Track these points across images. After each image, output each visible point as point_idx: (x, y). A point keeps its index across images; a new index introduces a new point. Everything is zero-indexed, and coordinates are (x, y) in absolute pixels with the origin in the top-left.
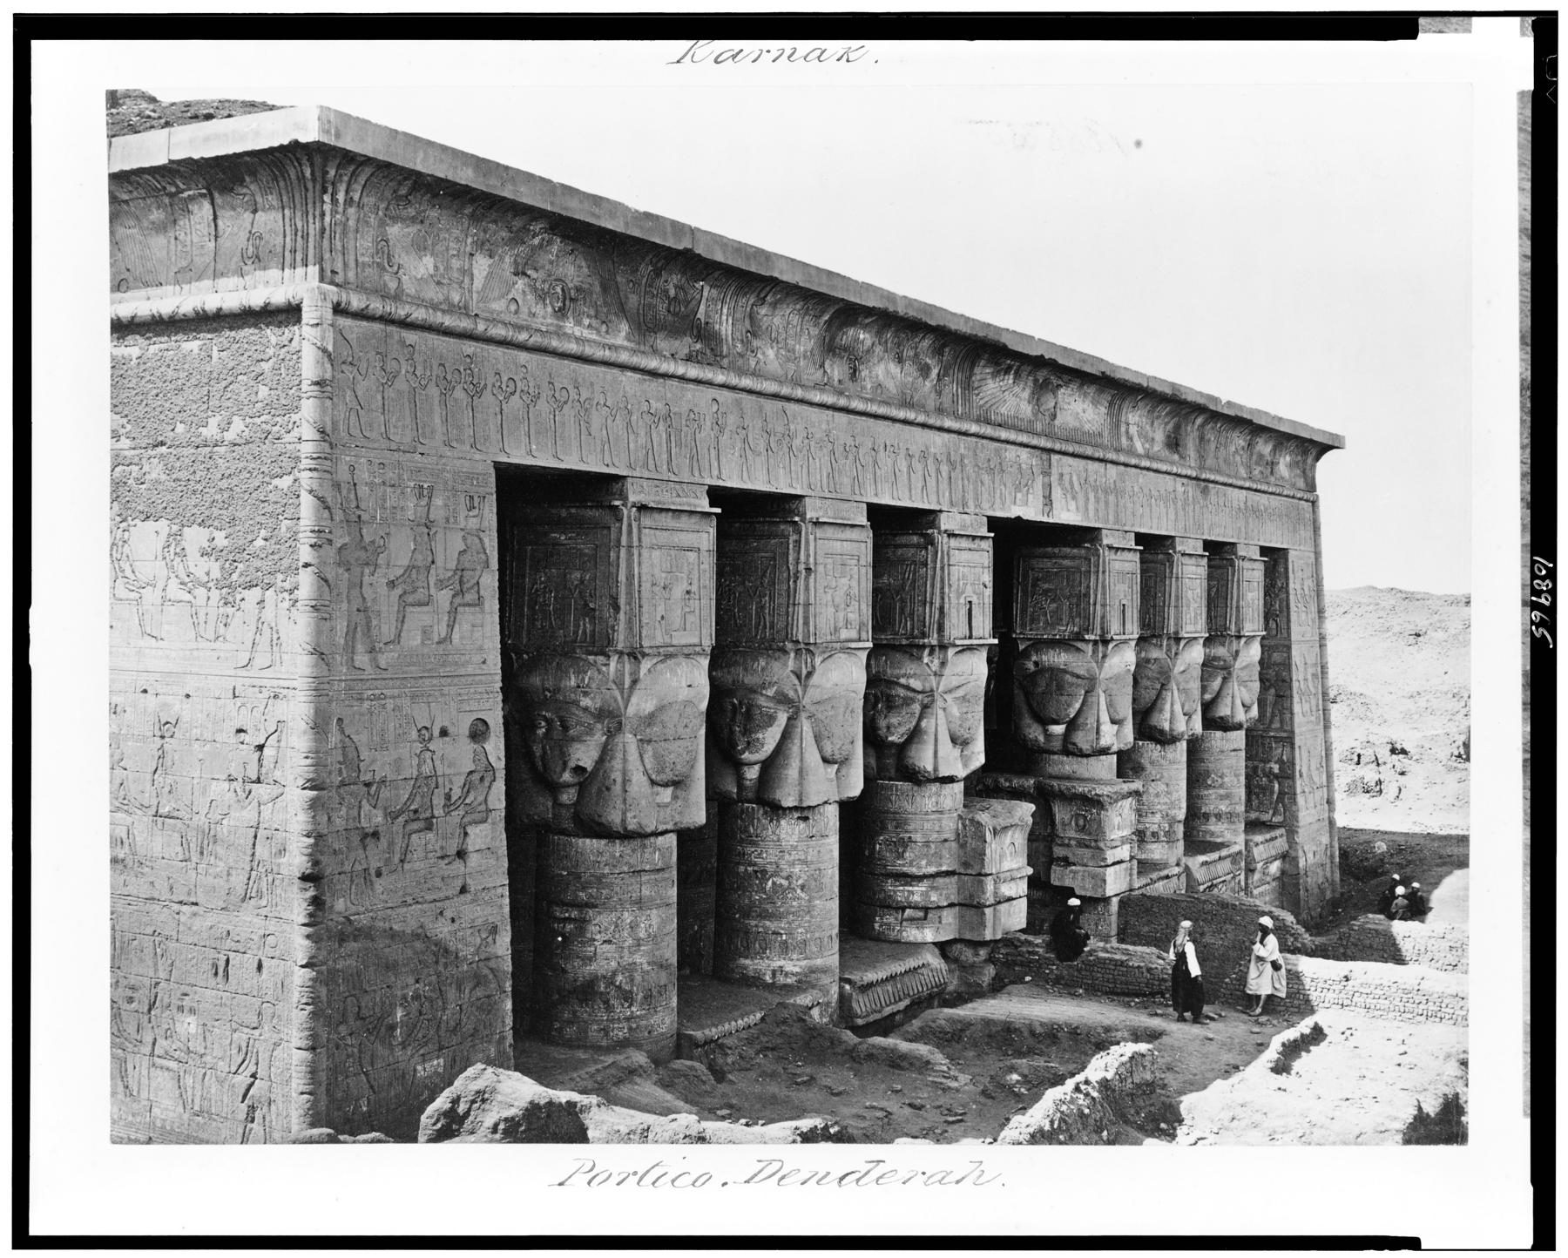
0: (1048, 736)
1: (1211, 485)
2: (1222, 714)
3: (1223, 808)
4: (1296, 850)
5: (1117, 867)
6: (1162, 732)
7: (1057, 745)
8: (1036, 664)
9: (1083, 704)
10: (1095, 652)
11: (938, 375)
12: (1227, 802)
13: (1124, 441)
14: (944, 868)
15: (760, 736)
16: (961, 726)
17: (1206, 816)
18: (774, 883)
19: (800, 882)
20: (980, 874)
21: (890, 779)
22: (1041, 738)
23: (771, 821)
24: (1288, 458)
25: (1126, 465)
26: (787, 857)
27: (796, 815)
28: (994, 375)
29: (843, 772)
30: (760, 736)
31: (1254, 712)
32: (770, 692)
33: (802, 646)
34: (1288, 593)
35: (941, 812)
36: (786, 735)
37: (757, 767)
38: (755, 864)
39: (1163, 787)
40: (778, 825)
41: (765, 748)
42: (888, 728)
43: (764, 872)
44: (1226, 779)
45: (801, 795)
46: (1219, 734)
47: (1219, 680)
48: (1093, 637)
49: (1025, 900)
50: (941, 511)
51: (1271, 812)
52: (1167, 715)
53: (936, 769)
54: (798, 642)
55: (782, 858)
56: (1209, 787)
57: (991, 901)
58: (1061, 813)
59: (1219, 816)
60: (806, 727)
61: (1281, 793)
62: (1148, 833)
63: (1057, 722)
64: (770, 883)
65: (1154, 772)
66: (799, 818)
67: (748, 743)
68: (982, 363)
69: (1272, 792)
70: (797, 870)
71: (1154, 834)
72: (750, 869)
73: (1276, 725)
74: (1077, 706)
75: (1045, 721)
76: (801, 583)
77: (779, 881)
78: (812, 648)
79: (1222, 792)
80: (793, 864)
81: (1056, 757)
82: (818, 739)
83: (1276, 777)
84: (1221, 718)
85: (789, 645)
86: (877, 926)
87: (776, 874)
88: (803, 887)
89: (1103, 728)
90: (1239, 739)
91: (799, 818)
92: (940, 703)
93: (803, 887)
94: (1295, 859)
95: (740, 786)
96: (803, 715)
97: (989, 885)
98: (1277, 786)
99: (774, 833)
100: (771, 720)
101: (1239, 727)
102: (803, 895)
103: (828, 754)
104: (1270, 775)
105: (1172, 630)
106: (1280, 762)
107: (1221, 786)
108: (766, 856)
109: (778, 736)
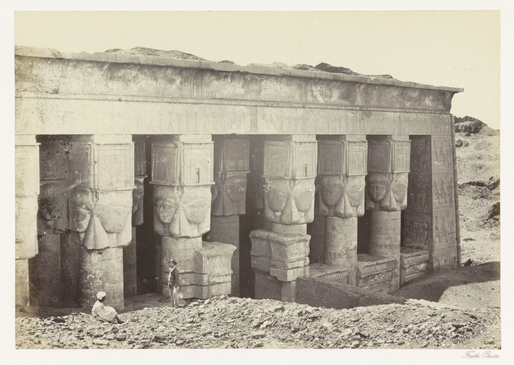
0: (275, 216)
1: (373, 112)
2: (386, 205)
3: (388, 242)
4: (432, 260)
5: (295, 270)
6: (340, 214)
7: (278, 220)
8: (270, 188)
9: (286, 203)
10: (290, 184)
11: (181, 82)
12: (389, 241)
13: (310, 99)
14: (187, 271)
15: (81, 222)
16: (191, 217)
17: (381, 246)
18: (90, 276)
19: (99, 276)
20: (201, 274)
21: (168, 237)
22: (273, 217)
23: (88, 254)
24: (431, 98)
25: (310, 108)
26: (94, 267)
27: (97, 252)
28: (218, 79)
29: (119, 236)
30: (81, 222)
31: (405, 203)
32: (84, 206)
33: (94, 190)
34: (431, 153)
35: (186, 250)
36: (90, 222)
37: (84, 234)
38: (84, 269)
39: (343, 236)
40: (91, 256)
41: (84, 227)
42: (164, 217)
43: (87, 272)
44: (389, 231)
45: (95, 245)
46: (386, 213)
47: (385, 191)
48: (288, 178)
49: (230, 283)
50: (181, 134)
51: (424, 243)
52: (343, 207)
53: (180, 234)
54: (91, 189)
55: (92, 267)
56: (382, 234)
57: (207, 284)
58: (273, 247)
59: (386, 246)
60: (97, 221)
61: (427, 236)
62: (337, 254)
63: (277, 211)
64: (88, 277)
65: (339, 230)
66: (98, 253)
67: (78, 225)
68: (208, 75)
69: (424, 235)
70: (98, 272)
71: (339, 255)
72: (83, 271)
73: (426, 208)
74: (284, 205)
75: (274, 211)
76: (92, 167)
77: (91, 276)
78: (97, 191)
79: (387, 236)
80: (96, 270)
81: (278, 225)
82: (103, 224)
83: (426, 229)
84: (386, 206)
85: (89, 190)
86: (164, 291)
87: (90, 273)
88: (100, 279)
89: (293, 214)
90: (397, 215)
91: (98, 253)
92: (181, 208)
93: (100, 279)
94: (432, 264)
95: (80, 240)
96: (95, 216)
97: (205, 278)
98: (426, 233)
99: (89, 258)
100: (84, 217)
101: (394, 210)
102: (100, 281)
103: (108, 230)
104: (423, 228)
105: (344, 172)
106: (428, 223)
107: (387, 234)
108: (88, 267)
109: (88, 223)
